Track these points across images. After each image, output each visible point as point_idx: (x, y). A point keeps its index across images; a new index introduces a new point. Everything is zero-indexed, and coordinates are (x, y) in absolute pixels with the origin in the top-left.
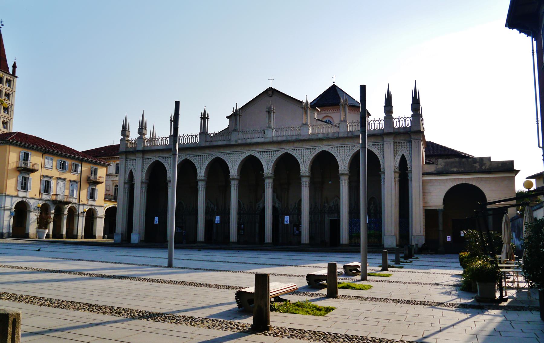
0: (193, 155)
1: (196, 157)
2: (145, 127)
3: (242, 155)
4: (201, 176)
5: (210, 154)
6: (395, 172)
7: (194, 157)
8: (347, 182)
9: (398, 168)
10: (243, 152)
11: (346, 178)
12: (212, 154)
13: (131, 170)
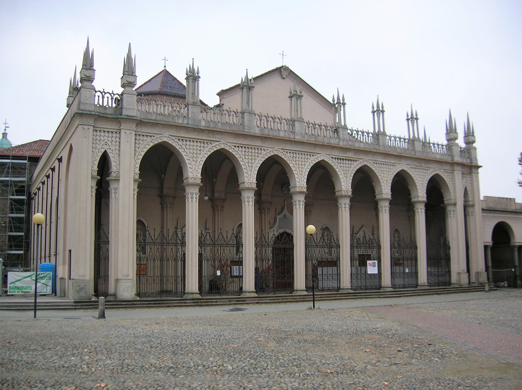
0: (235, 145)
1: (240, 149)
2: (456, 130)
3: (312, 158)
4: (251, 181)
5: (264, 148)
6: (92, 178)
7: (237, 148)
8: (423, 211)
9: (96, 171)
10: (313, 154)
11: (347, 201)
12: (267, 149)
13: (105, 152)
